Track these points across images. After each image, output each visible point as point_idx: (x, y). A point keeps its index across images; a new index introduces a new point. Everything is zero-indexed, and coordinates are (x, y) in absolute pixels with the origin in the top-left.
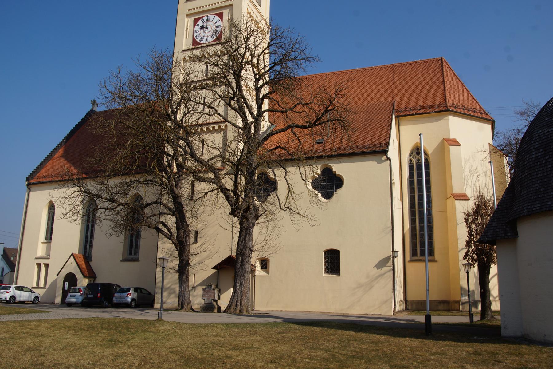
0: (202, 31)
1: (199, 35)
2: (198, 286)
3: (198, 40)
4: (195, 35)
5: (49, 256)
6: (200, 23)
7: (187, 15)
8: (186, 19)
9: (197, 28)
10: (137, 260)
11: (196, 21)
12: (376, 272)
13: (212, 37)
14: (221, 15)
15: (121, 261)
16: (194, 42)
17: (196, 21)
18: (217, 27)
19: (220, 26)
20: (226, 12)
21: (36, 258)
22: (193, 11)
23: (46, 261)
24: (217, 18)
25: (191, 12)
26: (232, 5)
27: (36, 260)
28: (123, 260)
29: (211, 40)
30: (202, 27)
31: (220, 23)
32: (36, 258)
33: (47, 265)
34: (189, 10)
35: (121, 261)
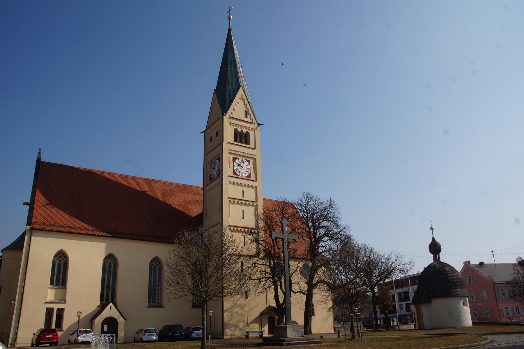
0: (239, 168)
1: (237, 169)
3: (237, 172)
4: (235, 168)
5: (65, 301)
6: (237, 161)
9: (235, 164)
10: (162, 307)
11: (234, 159)
12: (328, 314)
14: (249, 162)
16: (235, 173)
17: (234, 159)
18: (248, 168)
19: (249, 169)
20: (252, 161)
21: (46, 303)
22: (232, 152)
23: (61, 306)
24: (247, 163)
25: (231, 151)
26: (255, 159)
27: (46, 304)
28: (149, 306)
29: (244, 175)
30: (239, 165)
31: (249, 167)
32: (46, 303)
33: (61, 311)
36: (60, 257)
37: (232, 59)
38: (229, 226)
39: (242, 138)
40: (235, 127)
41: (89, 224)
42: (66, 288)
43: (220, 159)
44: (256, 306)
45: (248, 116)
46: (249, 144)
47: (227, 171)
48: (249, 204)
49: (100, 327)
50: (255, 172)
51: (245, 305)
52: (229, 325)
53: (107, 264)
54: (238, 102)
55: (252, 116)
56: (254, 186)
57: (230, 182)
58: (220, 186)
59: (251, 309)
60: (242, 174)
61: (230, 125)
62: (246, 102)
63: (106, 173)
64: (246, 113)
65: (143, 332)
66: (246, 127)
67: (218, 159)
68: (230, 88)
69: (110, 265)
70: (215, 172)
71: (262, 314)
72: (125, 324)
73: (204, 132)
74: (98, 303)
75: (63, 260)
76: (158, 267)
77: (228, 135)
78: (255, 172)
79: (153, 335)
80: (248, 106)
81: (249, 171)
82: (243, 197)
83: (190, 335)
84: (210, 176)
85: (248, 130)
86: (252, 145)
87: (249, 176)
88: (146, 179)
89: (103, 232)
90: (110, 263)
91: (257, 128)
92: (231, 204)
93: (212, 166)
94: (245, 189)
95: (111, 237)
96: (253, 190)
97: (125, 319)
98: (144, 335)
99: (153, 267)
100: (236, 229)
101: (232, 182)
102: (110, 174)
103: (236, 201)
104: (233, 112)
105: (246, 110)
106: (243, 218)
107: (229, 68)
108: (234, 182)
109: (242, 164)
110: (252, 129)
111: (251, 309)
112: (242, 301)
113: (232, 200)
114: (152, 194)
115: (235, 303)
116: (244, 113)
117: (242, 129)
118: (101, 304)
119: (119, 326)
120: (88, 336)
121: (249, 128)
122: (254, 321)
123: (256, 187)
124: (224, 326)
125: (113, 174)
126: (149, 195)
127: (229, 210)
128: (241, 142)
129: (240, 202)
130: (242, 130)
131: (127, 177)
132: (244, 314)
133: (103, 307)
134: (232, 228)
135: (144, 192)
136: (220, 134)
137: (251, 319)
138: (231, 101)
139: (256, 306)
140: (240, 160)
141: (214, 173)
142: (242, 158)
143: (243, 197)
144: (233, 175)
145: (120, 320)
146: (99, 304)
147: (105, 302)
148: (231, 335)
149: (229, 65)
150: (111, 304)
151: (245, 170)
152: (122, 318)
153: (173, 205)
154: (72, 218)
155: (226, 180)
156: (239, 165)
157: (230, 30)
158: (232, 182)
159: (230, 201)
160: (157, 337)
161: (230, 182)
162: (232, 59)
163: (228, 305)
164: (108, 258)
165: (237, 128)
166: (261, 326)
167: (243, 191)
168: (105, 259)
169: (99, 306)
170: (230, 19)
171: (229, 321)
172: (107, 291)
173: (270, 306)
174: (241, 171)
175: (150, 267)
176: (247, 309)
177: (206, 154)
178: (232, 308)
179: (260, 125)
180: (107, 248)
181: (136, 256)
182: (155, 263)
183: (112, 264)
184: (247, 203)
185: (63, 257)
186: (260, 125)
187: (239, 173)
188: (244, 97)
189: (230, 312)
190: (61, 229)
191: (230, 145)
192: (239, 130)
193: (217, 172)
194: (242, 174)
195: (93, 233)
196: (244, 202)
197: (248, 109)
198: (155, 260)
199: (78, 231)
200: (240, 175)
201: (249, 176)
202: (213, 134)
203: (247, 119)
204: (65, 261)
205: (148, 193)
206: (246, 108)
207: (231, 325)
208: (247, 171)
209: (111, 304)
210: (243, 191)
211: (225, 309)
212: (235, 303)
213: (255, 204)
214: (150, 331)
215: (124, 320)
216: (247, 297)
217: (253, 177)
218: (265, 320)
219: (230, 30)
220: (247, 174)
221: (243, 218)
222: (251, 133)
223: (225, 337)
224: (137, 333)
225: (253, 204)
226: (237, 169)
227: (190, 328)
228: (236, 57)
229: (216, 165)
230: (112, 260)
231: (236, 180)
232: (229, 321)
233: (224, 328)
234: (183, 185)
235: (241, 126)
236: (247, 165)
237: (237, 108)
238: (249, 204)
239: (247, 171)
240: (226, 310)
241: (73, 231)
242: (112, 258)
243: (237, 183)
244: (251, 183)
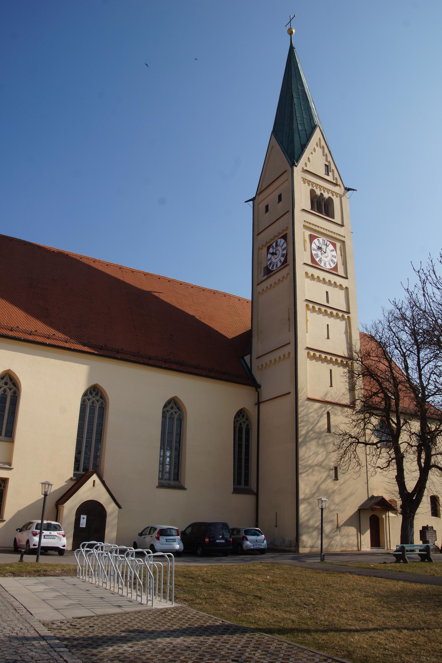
0: (319, 253)
1: (317, 255)
2: (342, 526)
3: (317, 260)
4: (314, 252)
5: (10, 464)
6: (316, 241)
7: (304, 226)
8: (304, 230)
9: (314, 246)
10: (182, 488)
11: (312, 238)
13: (329, 264)
14: (334, 245)
15: (157, 487)
17: (312, 238)
18: (333, 256)
20: (338, 245)
24: (331, 247)
28: (161, 486)
29: (328, 267)
31: (334, 253)
34: (305, 221)
35: (157, 487)
36: (6, 384)
37: (300, 88)
38: (308, 348)
39: (322, 206)
40: (310, 187)
41: (58, 330)
42: (12, 441)
43: (288, 236)
44: (351, 495)
45: (330, 174)
46: (334, 218)
47: (302, 256)
48: (337, 314)
49: (73, 519)
50: (345, 264)
51: (334, 492)
52: (308, 527)
53: (89, 403)
54: (314, 150)
55: (336, 175)
56: (344, 287)
57: (306, 273)
58: (288, 281)
59: (344, 500)
60: (325, 264)
61: (305, 183)
62: (326, 151)
63: (88, 259)
64: (327, 167)
65: (155, 534)
66: (328, 191)
67: (285, 237)
68: (300, 128)
69: (94, 404)
70: (277, 260)
71: (361, 510)
72: (119, 517)
73: (253, 200)
74: (68, 472)
75: (10, 389)
76: (176, 416)
77: (302, 200)
78: (345, 264)
79: (174, 540)
80: (329, 159)
81: (335, 260)
82: (328, 302)
83: (241, 545)
84: (267, 268)
85: (330, 195)
86: (338, 219)
87: (336, 268)
88: (152, 275)
89: (84, 346)
90: (93, 403)
91: (344, 194)
92: (309, 312)
93: (271, 250)
94: (330, 289)
95: (97, 355)
96: (342, 293)
97: (119, 507)
98: (158, 538)
99: (168, 415)
100: (318, 354)
101: (310, 275)
102: (95, 261)
103: (317, 307)
104: (308, 163)
105: (327, 164)
106: (328, 338)
107: (295, 100)
108: (312, 275)
109: (324, 247)
110: (337, 194)
111: (344, 500)
112: (330, 484)
113: (311, 305)
114: (162, 297)
115: (318, 488)
116: (324, 168)
117: (322, 192)
118: (74, 475)
119: (108, 519)
120: (54, 537)
121: (333, 192)
122: (348, 523)
123: (347, 288)
124: (300, 528)
125: (99, 261)
126: (158, 298)
127: (307, 321)
128: (320, 212)
129: (323, 309)
130: (321, 194)
131: (121, 268)
132: (332, 507)
133: (79, 481)
134: (312, 353)
135: (149, 293)
136: (287, 198)
137: (344, 517)
138: (303, 147)
139: (351, 495)
140: (321, 240)
141: (274, 260)
142: (324, 239)
143: (328, 302)
144: (311, 264)
145: (111, 508)
146: (72, 475)
147: (81, 472)
148: (312, 547)
149: (295, 95)
150: (95, 477)
151: (329, 257)
152: (114, 504)
153: (197, 317)
154: (30, 318)
155: (301, 271)
156: (319, 248)
157: (292, 49)
158: (310, 275)
159: (307, 306)
160: (182, 544)
161: (306, 273)
162: (300, 88)
163: (307, 491)
164: (91, 393)
165: (314, 188)
166: (360, 531)
167: (327, 292)
168: (85, 394)
169: (71, 479)
170: (291, 33)
171: (308, 520)
172: (86, 453)
173: (373, 497)
174: (324, 259)
175: (164, 416)
176: (337, 499)
177: (256, 233)
178: (313, 495)
179: (348, 190)
180: (90, 375)
181: (140, 392)
182: (172, 408)
183: (98, 405)
184: (335, 312)
185: (10, 385)
186: (348, 190)
187: (320, 261)
188: (323, 143)
189: (310, 504)
190: (11, 334)
191: (305, 214)
192: (318, 192)
193: (282, 259)
194: (325, 264)
195: (67, 345)
196: (329, 311)
197: (329, 162)
198: (172, 404)
199: (39, 339)
200: (322, 264)
201: (336, 268)
202: (270, 198)
203: (330, 178)
204: (15, 393)
205: (156, 294)
206: (327, 160)
207: (311, 527)
208: (332, 260)
209: (95, 477)
210: (327, 293)
211: (301, 496)
212: (318, 488)
213: (346, 316)
214: (163, 533)
215: (117, 507)
216: (336, 478)
217: (341, 272)
218: (366, 522)
219: (292, 49)
220: (333, 266)
221: (328, 338)
222: (336, 201)
223: (302, 550)
224: (141, 534)
225: (343, 316)
226: (317, 255)
227: (239, 531)
228: (305, 86)
229: (279, 248)
230: (98, 398)
231: (317, 273)
232: (308, 520)
233: (300, 532)
234: (210, 291)
235: (321, 187)
236: (332, 251)
237: (313, 158)
238: (337, 314)
239: (332, 260)
240: (304, 499)
241: (31, 338)
242: (97, 394)
243: (318, 277)
244: (339, 281)
